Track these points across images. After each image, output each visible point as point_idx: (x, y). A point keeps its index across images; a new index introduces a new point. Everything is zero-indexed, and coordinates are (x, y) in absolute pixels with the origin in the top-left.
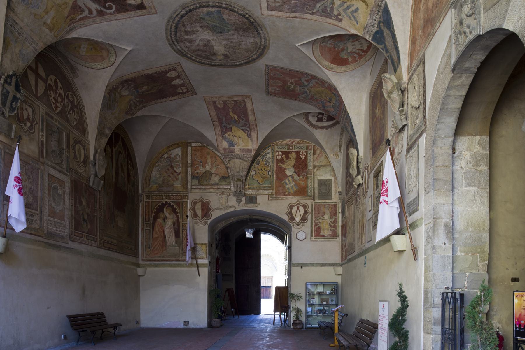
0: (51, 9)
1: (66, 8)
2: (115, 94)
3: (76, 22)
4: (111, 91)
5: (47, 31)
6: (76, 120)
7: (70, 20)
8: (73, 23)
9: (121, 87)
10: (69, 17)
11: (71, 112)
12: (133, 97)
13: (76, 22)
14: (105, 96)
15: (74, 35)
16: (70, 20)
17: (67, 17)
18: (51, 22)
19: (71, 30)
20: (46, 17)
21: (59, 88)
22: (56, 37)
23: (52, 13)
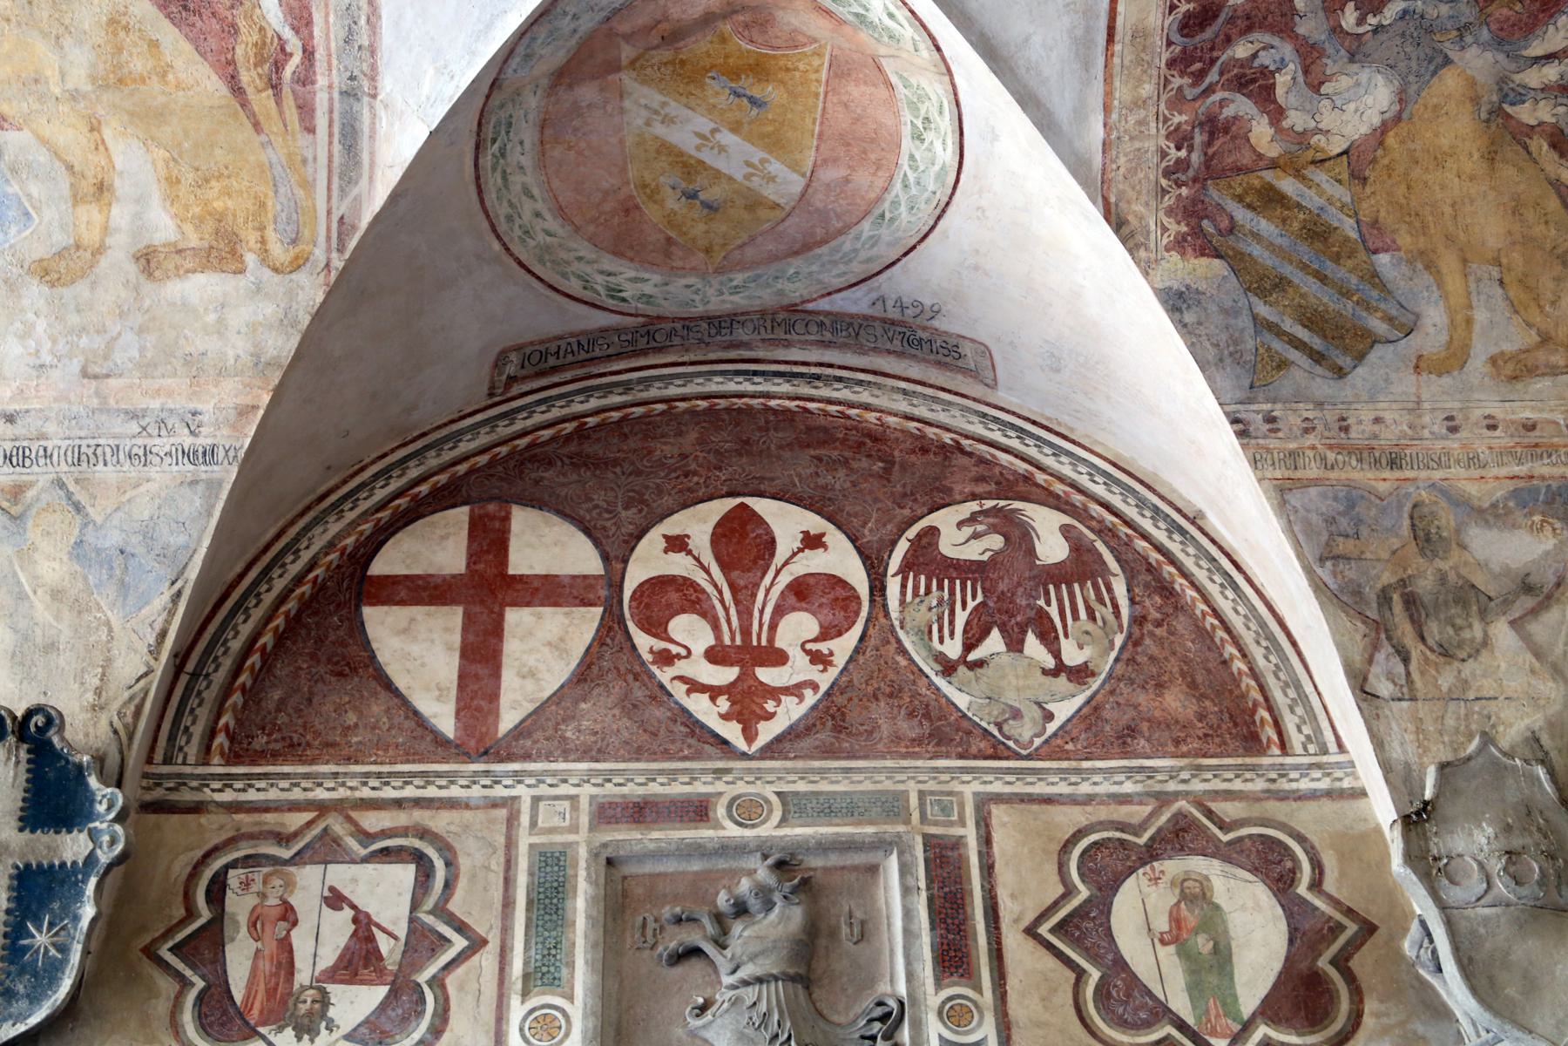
0: (100, 145)
1: (154, 45)
2: (1270, 199)
3: (308, 53)
4: (1192, 212)
5: (201, 287)
6: (1080, 674)
7: (276, 87)
8: (305, 78)
9: (1241, 106)
10: (246, 77)
11: (994, 642)
12: (1477, 62)
13: (308, 53)
14: (1176, 302)
15: (400, 136)
16: (276, 87)
17: (237, 90)
18: (180, 219)
19: (350, 137)
20: (120, 215)
21: (786, 542)
22: (297, 264)
23: (132, 161)
